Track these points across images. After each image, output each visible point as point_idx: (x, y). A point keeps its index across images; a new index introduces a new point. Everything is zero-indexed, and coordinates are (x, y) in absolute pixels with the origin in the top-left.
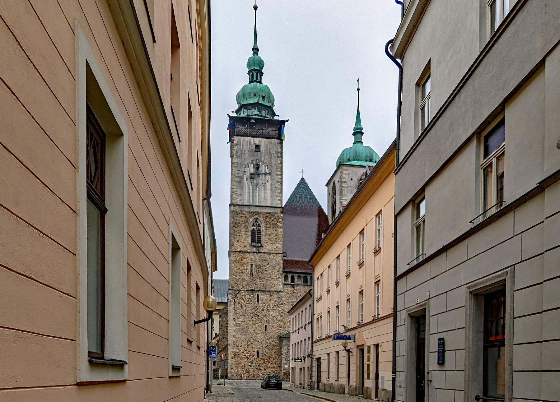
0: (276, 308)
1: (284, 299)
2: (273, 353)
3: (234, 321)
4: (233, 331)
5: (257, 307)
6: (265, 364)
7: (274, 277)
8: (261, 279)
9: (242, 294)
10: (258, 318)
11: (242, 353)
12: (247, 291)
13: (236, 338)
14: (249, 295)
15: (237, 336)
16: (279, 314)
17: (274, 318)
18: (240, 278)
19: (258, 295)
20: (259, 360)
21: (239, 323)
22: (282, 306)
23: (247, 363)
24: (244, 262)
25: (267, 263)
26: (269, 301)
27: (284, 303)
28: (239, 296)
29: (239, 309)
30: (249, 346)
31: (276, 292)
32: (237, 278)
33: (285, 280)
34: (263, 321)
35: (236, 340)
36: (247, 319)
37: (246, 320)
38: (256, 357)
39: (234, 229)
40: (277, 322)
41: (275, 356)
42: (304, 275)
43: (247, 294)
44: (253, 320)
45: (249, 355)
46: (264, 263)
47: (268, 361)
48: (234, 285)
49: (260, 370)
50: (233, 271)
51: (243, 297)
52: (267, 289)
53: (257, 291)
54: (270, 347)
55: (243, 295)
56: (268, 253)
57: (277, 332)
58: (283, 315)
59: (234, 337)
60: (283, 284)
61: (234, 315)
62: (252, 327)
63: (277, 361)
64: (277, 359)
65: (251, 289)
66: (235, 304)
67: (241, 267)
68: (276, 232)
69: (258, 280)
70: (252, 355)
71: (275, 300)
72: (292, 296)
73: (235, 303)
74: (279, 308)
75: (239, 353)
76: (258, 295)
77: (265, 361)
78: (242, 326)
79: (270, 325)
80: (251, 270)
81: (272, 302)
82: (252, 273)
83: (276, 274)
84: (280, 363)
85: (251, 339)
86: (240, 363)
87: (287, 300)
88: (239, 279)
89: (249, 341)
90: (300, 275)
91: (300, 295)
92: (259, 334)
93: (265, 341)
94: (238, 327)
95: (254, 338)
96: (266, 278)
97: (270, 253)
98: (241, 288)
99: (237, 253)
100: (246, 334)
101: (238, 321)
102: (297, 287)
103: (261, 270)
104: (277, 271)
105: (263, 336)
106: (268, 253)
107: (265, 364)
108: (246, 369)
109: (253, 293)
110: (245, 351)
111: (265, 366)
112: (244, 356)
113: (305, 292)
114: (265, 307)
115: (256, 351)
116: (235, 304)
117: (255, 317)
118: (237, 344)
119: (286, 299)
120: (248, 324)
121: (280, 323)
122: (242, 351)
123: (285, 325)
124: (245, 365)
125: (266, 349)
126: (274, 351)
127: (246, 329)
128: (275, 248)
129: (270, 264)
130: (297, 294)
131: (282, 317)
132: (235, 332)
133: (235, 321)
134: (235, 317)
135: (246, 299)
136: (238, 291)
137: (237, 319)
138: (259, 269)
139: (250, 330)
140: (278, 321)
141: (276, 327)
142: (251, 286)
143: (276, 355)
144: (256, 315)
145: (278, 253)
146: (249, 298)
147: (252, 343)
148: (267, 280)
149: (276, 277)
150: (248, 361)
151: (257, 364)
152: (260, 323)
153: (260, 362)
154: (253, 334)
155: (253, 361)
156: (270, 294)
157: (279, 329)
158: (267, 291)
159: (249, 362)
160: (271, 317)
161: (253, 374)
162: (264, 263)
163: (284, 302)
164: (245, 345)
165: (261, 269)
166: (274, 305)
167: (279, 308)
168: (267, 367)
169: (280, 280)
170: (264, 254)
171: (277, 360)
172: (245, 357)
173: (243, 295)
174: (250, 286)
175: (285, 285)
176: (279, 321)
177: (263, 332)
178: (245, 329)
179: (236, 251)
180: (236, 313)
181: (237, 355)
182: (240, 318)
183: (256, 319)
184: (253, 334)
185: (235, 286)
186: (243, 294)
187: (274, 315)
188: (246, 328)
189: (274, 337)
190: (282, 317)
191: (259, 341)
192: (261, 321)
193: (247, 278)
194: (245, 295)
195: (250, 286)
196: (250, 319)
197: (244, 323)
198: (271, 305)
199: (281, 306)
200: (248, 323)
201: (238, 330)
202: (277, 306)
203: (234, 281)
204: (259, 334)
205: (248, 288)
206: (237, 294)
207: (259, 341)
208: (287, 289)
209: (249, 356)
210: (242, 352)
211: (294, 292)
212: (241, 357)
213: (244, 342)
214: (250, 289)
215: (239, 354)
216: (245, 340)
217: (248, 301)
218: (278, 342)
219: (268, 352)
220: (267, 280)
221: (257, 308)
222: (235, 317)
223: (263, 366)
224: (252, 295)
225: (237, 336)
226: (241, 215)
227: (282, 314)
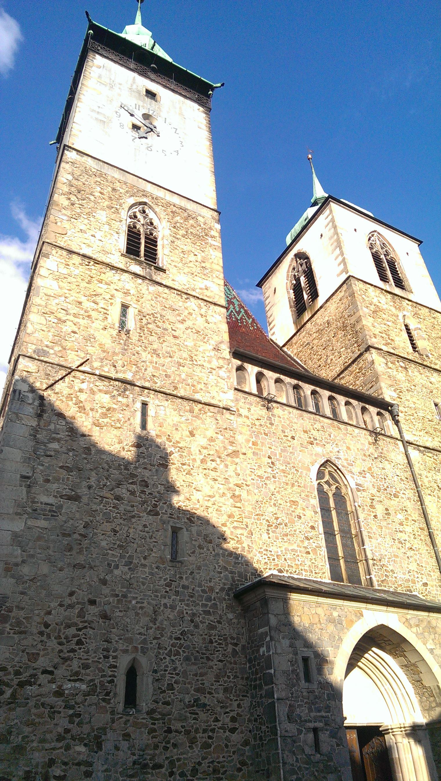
0: (214, 464)
1: (240, 439)
2: (211, 677)
3: (24, 490)
4: (8, 537)
6: (174, 753)
7: (205, 364)
8: (158, 355)
9: (77, 385)
10: (143, 492)
11: (43, 679)
12: (102, 377)
13: (19, 579)
14: (108, 396)
15: (25, 570)
16: (229, 489)
17: (209, 504)
18: (76, 329)
19: (145, 405)
20: (135, 724)
21: (51, 500)
22: (237, 460)
23: (68, 748)
24: (99, 291)
25: (180, 318)
26: (188, 433)
27: (245, 454)
28: (66, 391)
29: (58, 440)
30: (91, 632)
31: (211, 408)
32: (68, 327)
33: (239, 383)
35: (20, 588)
36: (90, 487)
37: (85, 490)
38: (121, 707)
39: (73, 198)
41: (221, 696)
42: (294, 382)
43: (100, 391)
44: (118, 498)
45: (84, 687)
46: (169, 315)
47: (188, 732)
48: (47, 346)
50: (54, 304)
51: (83, 397)
54: (197, 640)
55: (81, 391)
56: (180, 292)
57: (226, 569)
58: (244, 494)
59: (7, 570)
60: (236, 389)
61: (27, 460)
62: (115, 531)
63: (233, 730)
64: (233, 719)
65: (120, 376)
66: (40, 416)
67: (83, 299)
68: (203, 254)
69: (145, 356)
70: (102, 684)
72: (266, 434)
73: (43, 411)
74: (226, 466)
75: (23, 677)
76: (145, 405)
77: (169, 731)
78: (62, 518)
79: (194, 529)
80: (123, 324)
81: (200, 440)
83: (207, 354)
84: (246, 743)
85: (106, 590)
86: (19, 749)
87: (253, 444)
88: (74, 332)
89: (92, 602)
90: (282, 377)
91: (293, 438)
92: (144, 566)
93: (173, 608)
94: (42, 523)
95: (119, 590)
97: (186, 294)
98: (78, 363)
99: (77, 259)
100: (81, 559)
101: (47, 492)
102: (278, 411)
103: (159, 331)
104: (212, 347)
105: (162, 582)
106: (180, 292)
107: (174, 753)
109: (127, 393)
110: (65, 659)
111: (172, 763)
112: (52, 700)
113: (305, 432)
116: (40, 416)
117: (131, 487)
118: (22, 613)
119: (248, 441)
120: (93, 513)
121: (235, 528)
122: (43, 662)
123: (255, 536)
124: (51, 763)
125: (177, 653)
126: (216, 666)
127: (84, 536)
128: (201, 289)
129: (189, 323)
130: (283, 432)
131: (238, 505)
132: (20, 544)
133: (29, 486)
134: (33, 469)
135: (97, 407)
136: (63, 373)
137: (41, 480)
138: (150, 326)
139: (104, 544)
140: (225, 517)
142: (119, 368)
143: (226, 690)
144: (133, 476)
145: (210, 302)
146: (107, 406)
147: (105, 616)
148: (180, 364)
149: (210, 362)
150: (75, 730)
152: (150, 517)
154: (117, 567)
155: (103, 730)
156: (191, 411)
158: (181, 398)
159: (81, 740)
162: (169, 315)
163: (244, 451)
164: (68, 626)
165: (158, 326)
166: (205, 452)
167: (226, 466)
169: (222, 373)
170: (166, 290)
171: (230, 725)
172: (59, 702)
173: (81, 391)
174: (115, 366)
175: (240, 394)
176: (230, 516)
177: (162, 560)
178: (76, 536)
179: (71, 252)
180: (41, 452)
181: (9, 692)
182: (57, 480)
183: (133, 493)
184: (117, 567)
185: (51, 351)
186: (84, 386)
187: (207, 490)
188: (82, 531)
189: (212, 589)
190: (238, 505)
191: (145, 604)
192: (156, 506)
194: (93, 392)
195: (115, 366)
196: (105, 493)
197: (73, 506)
198: (194, 449)
199: (233, 462)
200: (94, 507)
201: (39, 538)
202: (218, 460)
203: (50, 334)
204: (144, 566)
205: (106, 369)
206: (56, 382)
207: (145, 604)
208: (249, 409)
209: (79, 698)
210: (45, 672)
211: (271, 424)
212: (31, 703)
213: (61, 605)
214: (113, 375)
215: (21, 685)
216: (71, 594)
217: (104, 415)
218: (230, 616)
219: (185, 672)
220: (180, 364)
222: (33, 469)
223: (161, 766)
224: (120, 399)
225: (25, 570)
226: (99, 180)
227: (237, 493)
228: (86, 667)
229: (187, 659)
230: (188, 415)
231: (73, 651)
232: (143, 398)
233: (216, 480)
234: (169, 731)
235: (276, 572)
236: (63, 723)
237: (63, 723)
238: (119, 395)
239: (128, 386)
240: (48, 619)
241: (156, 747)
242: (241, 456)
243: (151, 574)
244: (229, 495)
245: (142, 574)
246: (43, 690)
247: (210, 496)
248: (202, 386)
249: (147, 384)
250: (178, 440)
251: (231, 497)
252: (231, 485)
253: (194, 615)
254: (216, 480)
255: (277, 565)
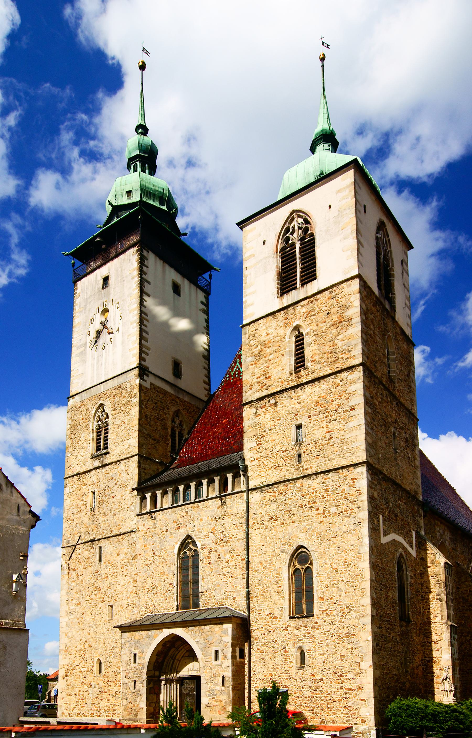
5: (97, 572)
26: (116, 555)
27: (140, 555)
34: (106, 598)
40: (128, 595)
49: (101, 700)
52: (114, 533)
53: (99, 540)
57: (128, 618)
71: (125, 550)
74: (132, 566)
81: (122, 556)
82: (93, 509)
89: (86, 641)
92: (100, 624)
96: (112, 513)
99: (75, 477)
107: (109, 688)
108: (82, 699)
110: (82, 661)
112: (79, 674)
114: (110, 569)
115: (96, 660)
122: (77, 663)
123: (141, 599)
141: (126, 606)
148: (114, 515)
151: (97, 689)
153: (101, 684)
157: (130, 611)
160: (119, 587)
161: (91, 710)
166: (123, 562)
167: (132, 566)
168: (112, 695)
184: (92, 627)
187: (122, 583)
192: (103, 598)
193: (86, 519)
202: (128, 564)
204: (100, 624)
209: (85, 673)
210: (77, 665)
221: (99, 573)
223: (106, 692)
224: (92, 550)
227: (135, 579)
228: (87, 663)
229: (114, 657)
230: (117, 544)
231: (83, 658)
232: (99, 546)
233: (126, 576)
234: (109, 681)
235: (149, 614)
236: (82, 680)
237: (82, 680)
238: (91, 549)
239: (94, 542)
240: (76, 649)
241: (105, 686)
242: (139, 557)
243: (103, 627)
244: (132, 581)
245: (100, 628)
246: (77, 671)
247: (124, 585)
248: (123, 523)
249: (100, 537)
250: (112, 561)
251: (133, 582)
252: (133, 576)
253: (116, 640)
254: (126, 576)
255: (151, 610)
